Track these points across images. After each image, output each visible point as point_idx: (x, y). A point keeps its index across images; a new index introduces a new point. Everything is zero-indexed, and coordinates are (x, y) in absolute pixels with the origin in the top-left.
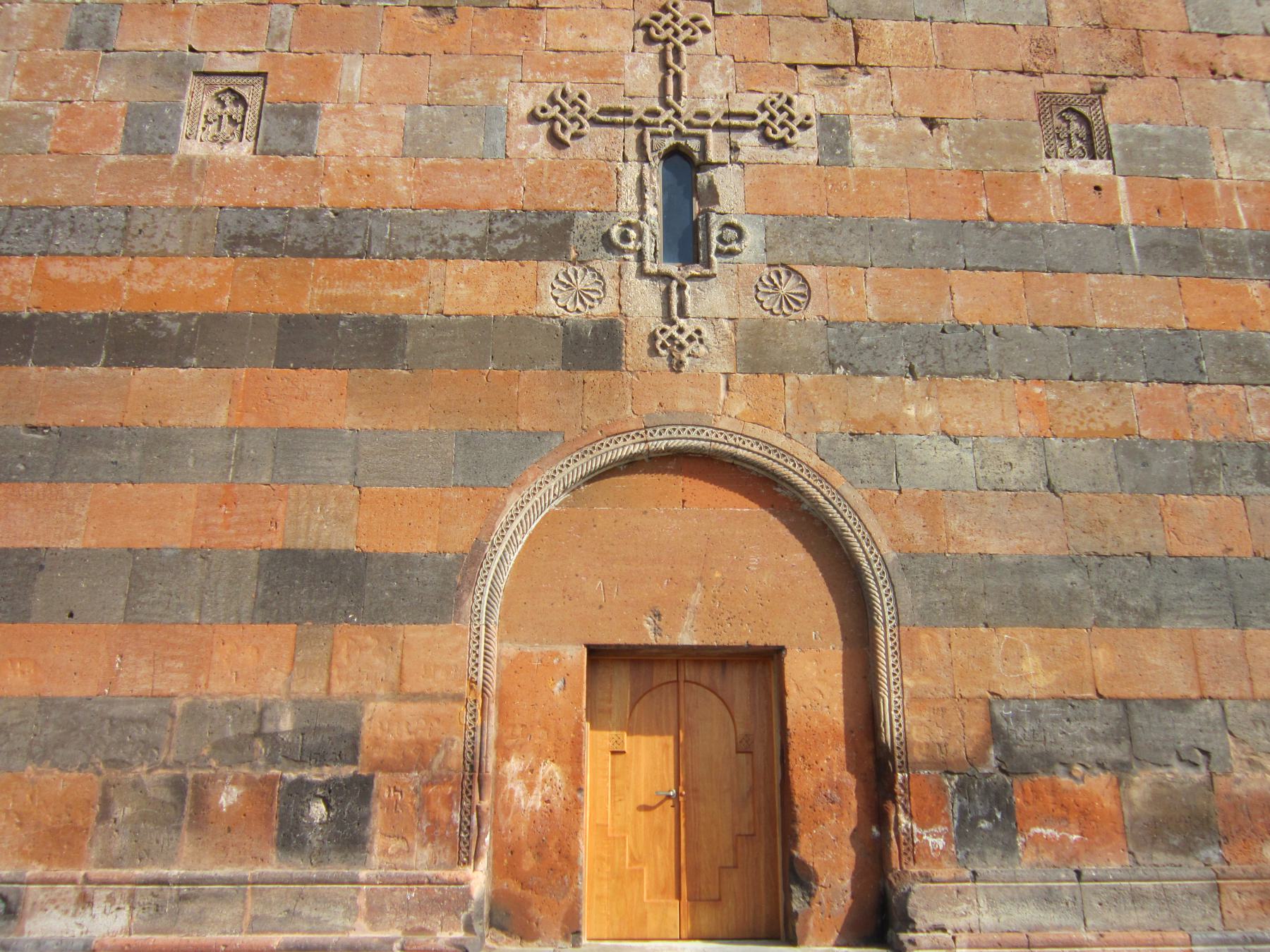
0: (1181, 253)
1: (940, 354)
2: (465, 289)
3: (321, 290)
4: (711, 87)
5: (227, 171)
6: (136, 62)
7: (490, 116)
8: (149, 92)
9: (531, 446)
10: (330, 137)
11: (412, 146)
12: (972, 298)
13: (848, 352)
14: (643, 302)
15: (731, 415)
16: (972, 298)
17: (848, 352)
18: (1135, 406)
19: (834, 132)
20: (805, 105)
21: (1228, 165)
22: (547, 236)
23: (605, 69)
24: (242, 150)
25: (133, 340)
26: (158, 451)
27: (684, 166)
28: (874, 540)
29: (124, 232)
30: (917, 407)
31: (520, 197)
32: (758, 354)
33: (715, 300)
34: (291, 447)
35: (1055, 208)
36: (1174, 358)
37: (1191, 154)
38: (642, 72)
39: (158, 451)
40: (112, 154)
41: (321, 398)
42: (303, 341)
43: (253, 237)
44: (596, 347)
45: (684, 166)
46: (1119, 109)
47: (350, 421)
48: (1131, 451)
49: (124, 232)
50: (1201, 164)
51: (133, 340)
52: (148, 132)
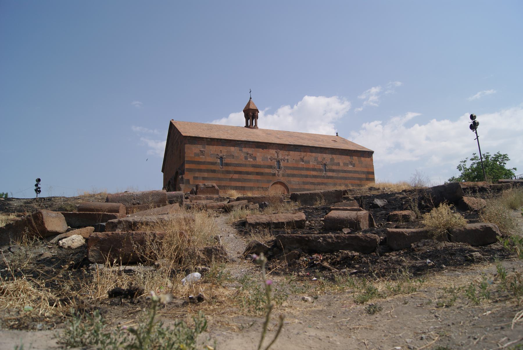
0: (307, 169)
1: (294, 176)
2: (267, 170)
3: (259, 170)
4: (280, 157)
5: (251, 161)
6: (244, 152)
7: (267, 158)
8: (246, 155)
9: (271, 181)
10: (257, 160)
11: (262, 160)
12: (296, 172)
13: (288, 175)
14: (277, 172)
15: (282, 179)
16: (296, 172)
17: (288, 175)
18: (305, 180)
19: (288, 160)
20: (286, 158)
21: (311, 163)
22: (270, 167)
23: (274, 155)
24: (252, 160)
25: (248, 173)
26: (250, 181)
27: (279, 162)
28: (290, 187)
29: (245, 165)
30: (292, 179)
31: (269, 164)
32: (283, 175)
33: (281, 172)
34: (258, 181)
35: (300, 166)
36: (306, 176)
37: (309, 162)
38: (276, 155)
39: (250, 181)
40: (244, 159)
41: (259, 177)
42: (258, 174)
43: (254, 166)
44: (274, 175)
45: (279, 162)
46: (305, 159)
47: (260, 179)
48: (304, 182)
49: (245, 165)
50: (309, 163)
51: (248, 173)
52: (246, 158)
